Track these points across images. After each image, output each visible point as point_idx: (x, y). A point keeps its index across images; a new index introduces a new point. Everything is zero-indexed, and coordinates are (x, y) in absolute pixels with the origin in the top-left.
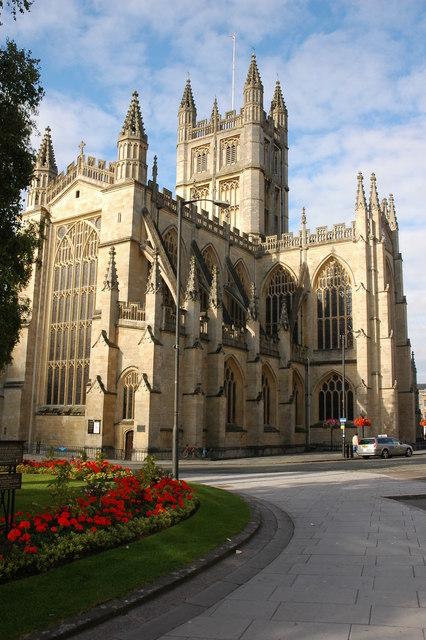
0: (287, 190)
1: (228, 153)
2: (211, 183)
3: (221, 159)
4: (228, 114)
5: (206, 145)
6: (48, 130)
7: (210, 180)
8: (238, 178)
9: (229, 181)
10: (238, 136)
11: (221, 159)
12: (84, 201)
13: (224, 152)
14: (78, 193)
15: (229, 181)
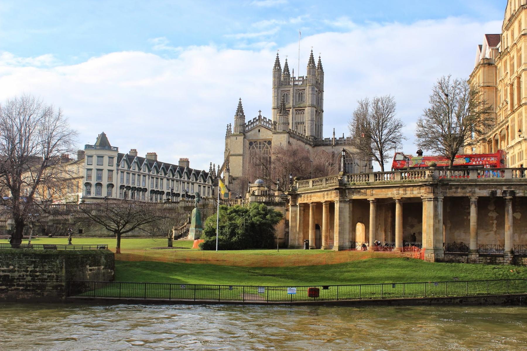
0: (323, 112)
1: (299, 96)
2: (291, 110)
3: (296, 99)
4: (299, 77)
5: (288, 90)
6: (240, 99)
7: (291, 108)
8: (304, 110)
9: (300, 110)
10: (304, 89)
11: (296, 99)
12: (262, 134)
13: (297, 95)
14: (259, 131)
15: (300, 110)
